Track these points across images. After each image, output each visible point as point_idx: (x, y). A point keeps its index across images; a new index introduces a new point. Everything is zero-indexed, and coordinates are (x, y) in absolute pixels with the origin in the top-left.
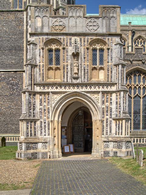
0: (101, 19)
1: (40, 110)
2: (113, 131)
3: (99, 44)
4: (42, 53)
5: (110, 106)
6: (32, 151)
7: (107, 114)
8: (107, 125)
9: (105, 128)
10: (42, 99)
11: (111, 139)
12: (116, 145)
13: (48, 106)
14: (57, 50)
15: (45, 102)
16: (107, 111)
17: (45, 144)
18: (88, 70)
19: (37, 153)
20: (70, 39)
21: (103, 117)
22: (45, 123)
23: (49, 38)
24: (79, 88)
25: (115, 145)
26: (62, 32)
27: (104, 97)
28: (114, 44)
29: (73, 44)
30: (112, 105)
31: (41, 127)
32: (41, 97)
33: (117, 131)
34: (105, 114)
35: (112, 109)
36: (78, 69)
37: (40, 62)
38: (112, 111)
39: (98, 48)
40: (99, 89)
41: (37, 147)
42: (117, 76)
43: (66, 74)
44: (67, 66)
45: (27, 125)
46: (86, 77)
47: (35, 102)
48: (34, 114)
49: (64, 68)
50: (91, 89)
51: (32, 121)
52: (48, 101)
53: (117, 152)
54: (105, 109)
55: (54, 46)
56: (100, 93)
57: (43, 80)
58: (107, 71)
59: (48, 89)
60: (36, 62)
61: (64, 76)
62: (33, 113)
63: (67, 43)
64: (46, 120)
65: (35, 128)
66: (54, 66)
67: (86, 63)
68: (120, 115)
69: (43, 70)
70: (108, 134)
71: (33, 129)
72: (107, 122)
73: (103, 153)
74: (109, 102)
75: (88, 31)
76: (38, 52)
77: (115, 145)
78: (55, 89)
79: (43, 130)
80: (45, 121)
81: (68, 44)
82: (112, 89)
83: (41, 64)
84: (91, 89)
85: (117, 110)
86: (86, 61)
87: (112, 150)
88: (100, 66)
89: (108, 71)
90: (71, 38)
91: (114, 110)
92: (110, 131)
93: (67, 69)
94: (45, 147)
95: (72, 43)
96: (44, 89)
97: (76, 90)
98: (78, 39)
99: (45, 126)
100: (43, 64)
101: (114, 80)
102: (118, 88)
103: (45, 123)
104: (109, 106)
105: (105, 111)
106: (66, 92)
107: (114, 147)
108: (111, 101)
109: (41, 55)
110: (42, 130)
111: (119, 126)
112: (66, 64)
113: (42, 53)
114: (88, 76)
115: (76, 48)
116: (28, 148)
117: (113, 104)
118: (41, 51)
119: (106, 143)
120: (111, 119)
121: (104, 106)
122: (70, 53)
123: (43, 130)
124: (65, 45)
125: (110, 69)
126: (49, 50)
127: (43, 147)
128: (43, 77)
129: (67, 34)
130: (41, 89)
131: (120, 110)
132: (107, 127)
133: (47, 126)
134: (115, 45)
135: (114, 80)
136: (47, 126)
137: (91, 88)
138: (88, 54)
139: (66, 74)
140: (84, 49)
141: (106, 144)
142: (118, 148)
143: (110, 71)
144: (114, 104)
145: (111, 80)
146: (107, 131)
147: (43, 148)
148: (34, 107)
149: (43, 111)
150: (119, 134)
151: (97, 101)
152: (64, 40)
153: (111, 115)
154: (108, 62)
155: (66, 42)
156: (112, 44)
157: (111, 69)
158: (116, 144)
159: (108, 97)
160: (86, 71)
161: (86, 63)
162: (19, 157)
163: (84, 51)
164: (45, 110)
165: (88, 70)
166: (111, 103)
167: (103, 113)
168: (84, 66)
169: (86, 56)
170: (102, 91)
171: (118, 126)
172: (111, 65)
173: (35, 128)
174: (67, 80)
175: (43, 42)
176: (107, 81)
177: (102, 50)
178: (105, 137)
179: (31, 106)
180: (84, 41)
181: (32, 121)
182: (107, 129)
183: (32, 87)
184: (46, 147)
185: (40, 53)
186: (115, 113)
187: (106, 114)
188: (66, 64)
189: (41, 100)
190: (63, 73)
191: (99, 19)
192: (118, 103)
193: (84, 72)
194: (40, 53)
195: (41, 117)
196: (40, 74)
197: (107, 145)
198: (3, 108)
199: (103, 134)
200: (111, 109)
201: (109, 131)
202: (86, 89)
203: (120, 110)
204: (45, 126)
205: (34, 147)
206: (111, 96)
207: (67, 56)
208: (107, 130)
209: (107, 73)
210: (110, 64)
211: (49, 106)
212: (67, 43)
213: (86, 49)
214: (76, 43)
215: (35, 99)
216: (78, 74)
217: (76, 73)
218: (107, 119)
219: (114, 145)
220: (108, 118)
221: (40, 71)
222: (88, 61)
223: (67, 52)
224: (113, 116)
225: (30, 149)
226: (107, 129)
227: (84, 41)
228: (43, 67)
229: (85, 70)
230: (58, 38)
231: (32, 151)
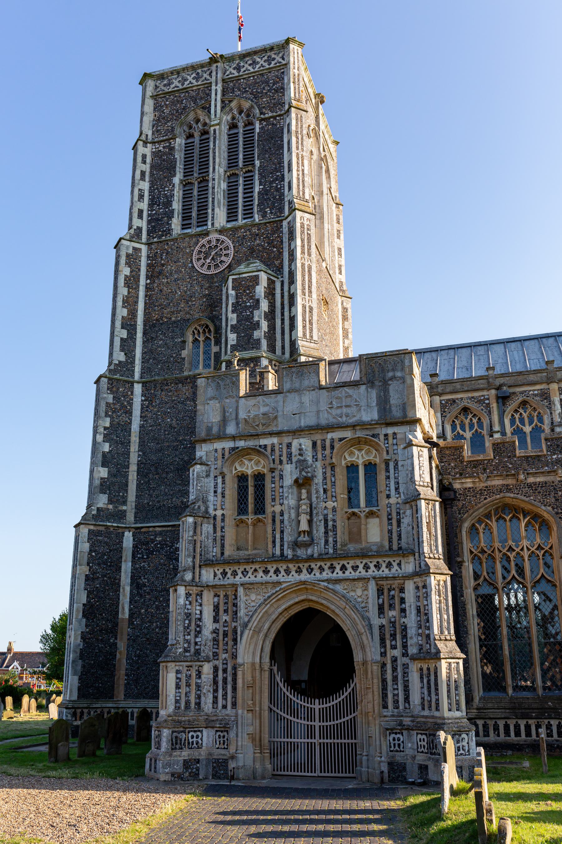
0: (363, 388)
1: (215, 635)
2: (415, 698)
3: (363, 452)
4: (220, 485)
5: (403, 620)
6: (185, 754)
7: (393, 643)
8: (395, 679)
9: (390, 688)
10: (218, 604)
11: (409, 723)
12: (425, 743)
13: (234, 624)
14: (259, 478)
15: (226, 611)
16: (393, 636)
17: (222, 734)
18: (334, 521)
19: (199, 760)
20: (289, 446)
21: (383, 654)
22: (225, 671)
23: (238, 448)
24: (313, 573)
25: (422, 743)
26: (269, 429)
27: (383, 594)
28: (402, 446)
29: (295, 456)
30: (405, 617)
31: (215, 682)
32: (216, 599)
33: (426, 698)
34: (388, 643)
35: (406, 627)
36: (310, 522)
37: (215, 510)
38: (409, 636)
39: (360, 462)
40: (367, 571)
41: (200, 742)
42: (415, 532)
43: (278, 536)
44: (282, 514)
45: (177, 678)
46: (331, 539)
47: (201, 612)
48: (197, 647)
49: (274, 521)
50: (344, 573)
51: (191, 666)
52: (235, 609)
53: (426, 767)
54: (387, 630)
55: (249, 465)
56: (370, 582)
57: (222, 554)
58: (385, 519)
59: (235, 578)
60: (207, 508)
61: (274, 542)
62: (196, 643)
63: (281, 456)
64: (227, 664)
65: (198, 687)
66: (250, 518)
67: (330, 504)
68: (428, 645)
69: (223, 528)
70: (401, 707)
71: (194, 687)
72: (394, 669)
73: (385, 768)
74: (397, 606)
75: (332, 420)
76: (212, 485)
77: (422, 743)
78: (251, 576)
79: (220, 692)
80: (225, 666)
81: (284, 458)
82: (403, 571)
83: (219, 513)
84: (344, 573)
85: (420, 631)
87: (414, 758)
88: (367, 510)
89: (389, 519)
90: (290, 444)
91: (412, 631)
92: (407, 699)
93: (282, 522)
94: (222, 742)
95: (293, 454)
96: (224, 578)
97: (305, 577)
98: (306, 443)
99: (225, 680)
100: (221, 512)
101: (408, 544)
102: (420, 567)
103: (225, 671)
104: (397, 619)
105: (388, 636)
106: (279, 583)
107: (419, 750)
108: (403, 606)
109: (219, 490)
110: (216, 691)
111: (429, 681)
112: (278, 509)
113: (220, 485)
114: (336, 537)
115: (302, 464)
116: (176, 744)
117: (408, 612)
118: (220, 480)
119: (393, 735)
120: (406, 660)
121: (384, 621)
122: (288, 481)
123: (220, 692)
124: (277, 461)
125: (394, 515)
126: (238, 476)
127: (218, 743)
128: (223, 546)
129: (279, 434)
130: (217, 578)
131: (427, 632)
132: (397, 684)
133: (229, 679)
134: (405, 448)
135: (408, 544)
136: (229, 679)
137: (346, 569)
138: (333, 479)
139: (278, 536)
140: (324, 467)
141: (394, 739)
142: (431, 754)
143: (394, 522)
144: (411, 613)
145: (399, 544)
146: (396, 698)
147: (217, 746)
148: (198, 626)
149: (221, 637)
150: (430, 707)
151: (363, 605)
152: (273, 450)
153: (405, 646)
154: (388, 496)
155: (277, 453)
156: (395, 447)
157: (398, 514)
158: (424, 739)
159: (392, 593)
160: (330, 523)
161: (330, 504)
162: (150, 770)
163: (325, 473)
164: (225, 634)
165: (334, 521)
166: (403, 611)
167: (383, 640)
168: (326, 512)
169: (329, 486)
170: (374, 578)
171: (425, 681)
172: (398, 503)
173: (198, 687)
174: (282, 550)
175: (223, 458)
176: (387, 547)
177: (370, 467)
178: (393, 716)
179: (189, 624)
180: (324, 448)
181: (191, 666)
182: (396, 692)
183: (194, 573)
184: (224, 744)
185: (216, 486)
186: (415, 640)
187: (391, 646)
188: (278, 509)
189: (216, 608)
191: (359, 388)
192: (422, 610)
193: (326, 526)
194: (216, 486)
195: (216, 655)
196: (215, 540)
197: (396, 742)
198: (154, 624)
199: (385, 707)
200: (405, 629)
201: (401, 698)
202: (333, 572)
203: (427, 632)
204: (225, 680)
205: (193, 742)
206: (402, 590)
207: (281, 490)
208: (398, 695)
209: (386, 528)
210: (393, 500)
211: (235, 624)
212: (281, 456)
213: (329, 469)
214: (301, 455)
215: (201, 605)
218: (394, 660)
219: (419, 743)
220: (396, 655)
221: (215, 532)
222: (334, 499)
223: (281, 477)
224: (413, 650)
225: (182, 749)
226: (396, 692)
227: (324, 448)
228: (223, 520)
229: (326, 521)
230: (260, 446)
231: (185, 754)
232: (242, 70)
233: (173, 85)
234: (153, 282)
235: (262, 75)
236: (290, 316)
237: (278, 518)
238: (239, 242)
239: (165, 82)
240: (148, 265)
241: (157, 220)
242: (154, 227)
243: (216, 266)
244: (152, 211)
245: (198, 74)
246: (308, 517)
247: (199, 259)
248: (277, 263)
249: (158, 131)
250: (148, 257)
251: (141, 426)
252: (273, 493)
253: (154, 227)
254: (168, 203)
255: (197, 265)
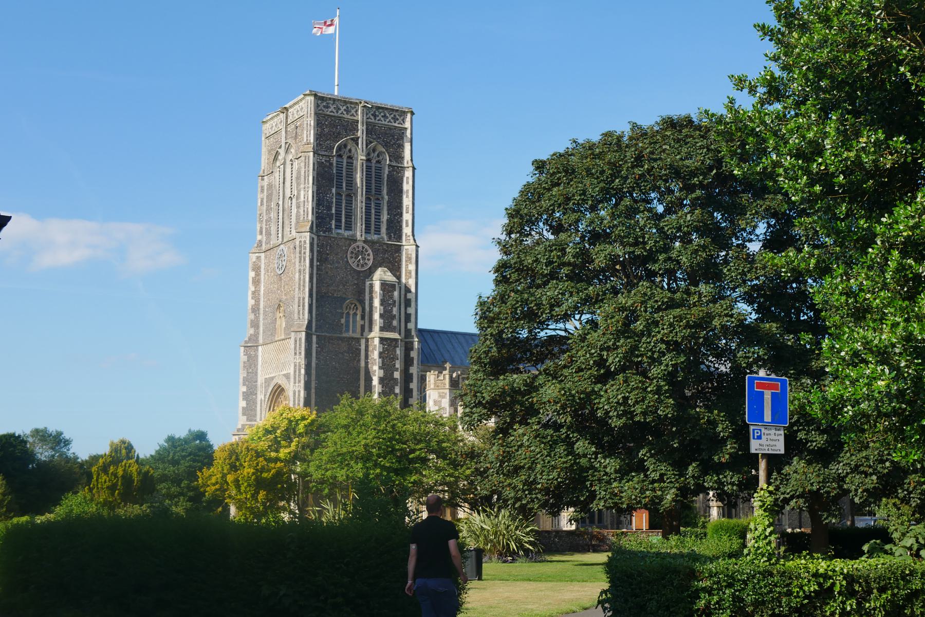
232: (378, 118)
233: (330, 110)
234: (321, 265)
235: (390, 129)
236: (406, 313)
238: (376, 253)
239: (324, 104)
240: (318, 251)
241: (322, 218)
242: (320, 223)
243: (362, 266)
244: (319, 209)
245: (347, 107)
247: (352, 257)
248: (398, 274)
249: (320, 145)
250: (318, 245)
251: (317, 364)
253: (320, 223)
254: (330, 208)
255: (350, 261)
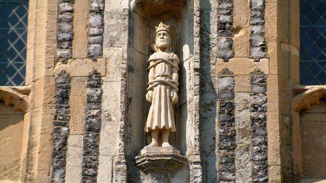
36: (178, 109)
49: (64, 97)
86: (240, 50)
112: (80, 68)
160: (243, 116)
188: (80, 68)
190: (50, 128)
207: (95, 19)
216: (177, 138)
217: (160, 133)
229: (229, 108)
237: (79, 94)
246: (175, 95)
252: (66, 27)
